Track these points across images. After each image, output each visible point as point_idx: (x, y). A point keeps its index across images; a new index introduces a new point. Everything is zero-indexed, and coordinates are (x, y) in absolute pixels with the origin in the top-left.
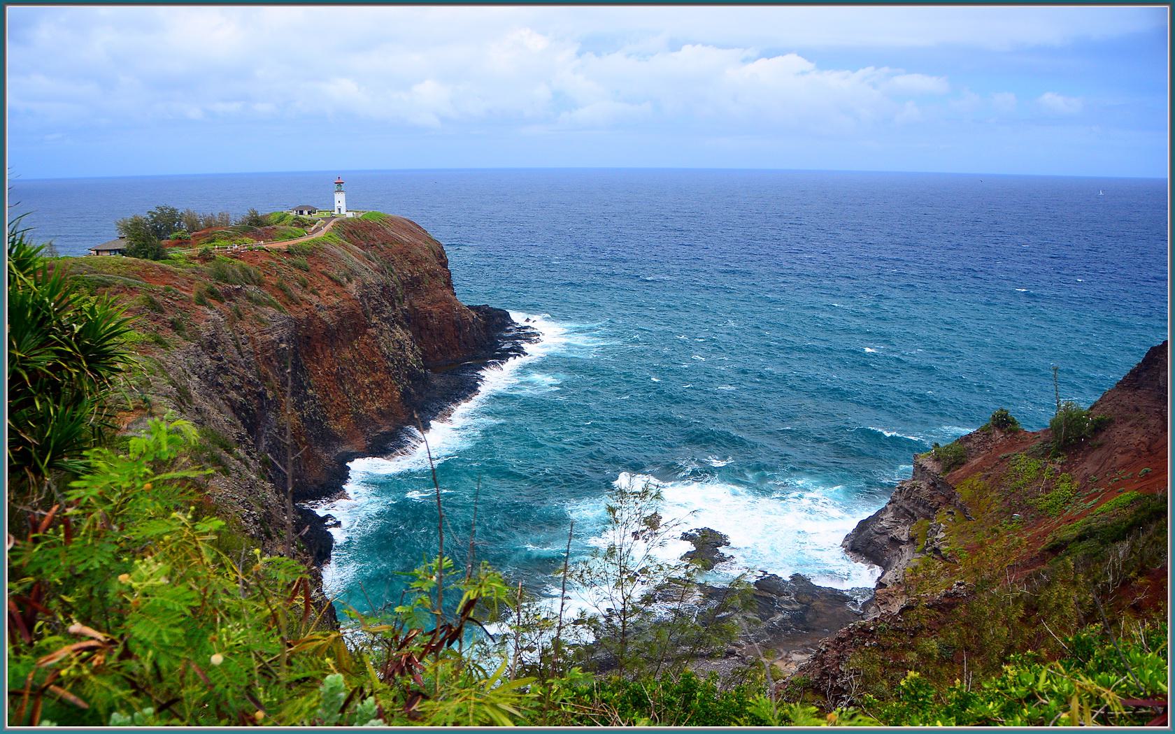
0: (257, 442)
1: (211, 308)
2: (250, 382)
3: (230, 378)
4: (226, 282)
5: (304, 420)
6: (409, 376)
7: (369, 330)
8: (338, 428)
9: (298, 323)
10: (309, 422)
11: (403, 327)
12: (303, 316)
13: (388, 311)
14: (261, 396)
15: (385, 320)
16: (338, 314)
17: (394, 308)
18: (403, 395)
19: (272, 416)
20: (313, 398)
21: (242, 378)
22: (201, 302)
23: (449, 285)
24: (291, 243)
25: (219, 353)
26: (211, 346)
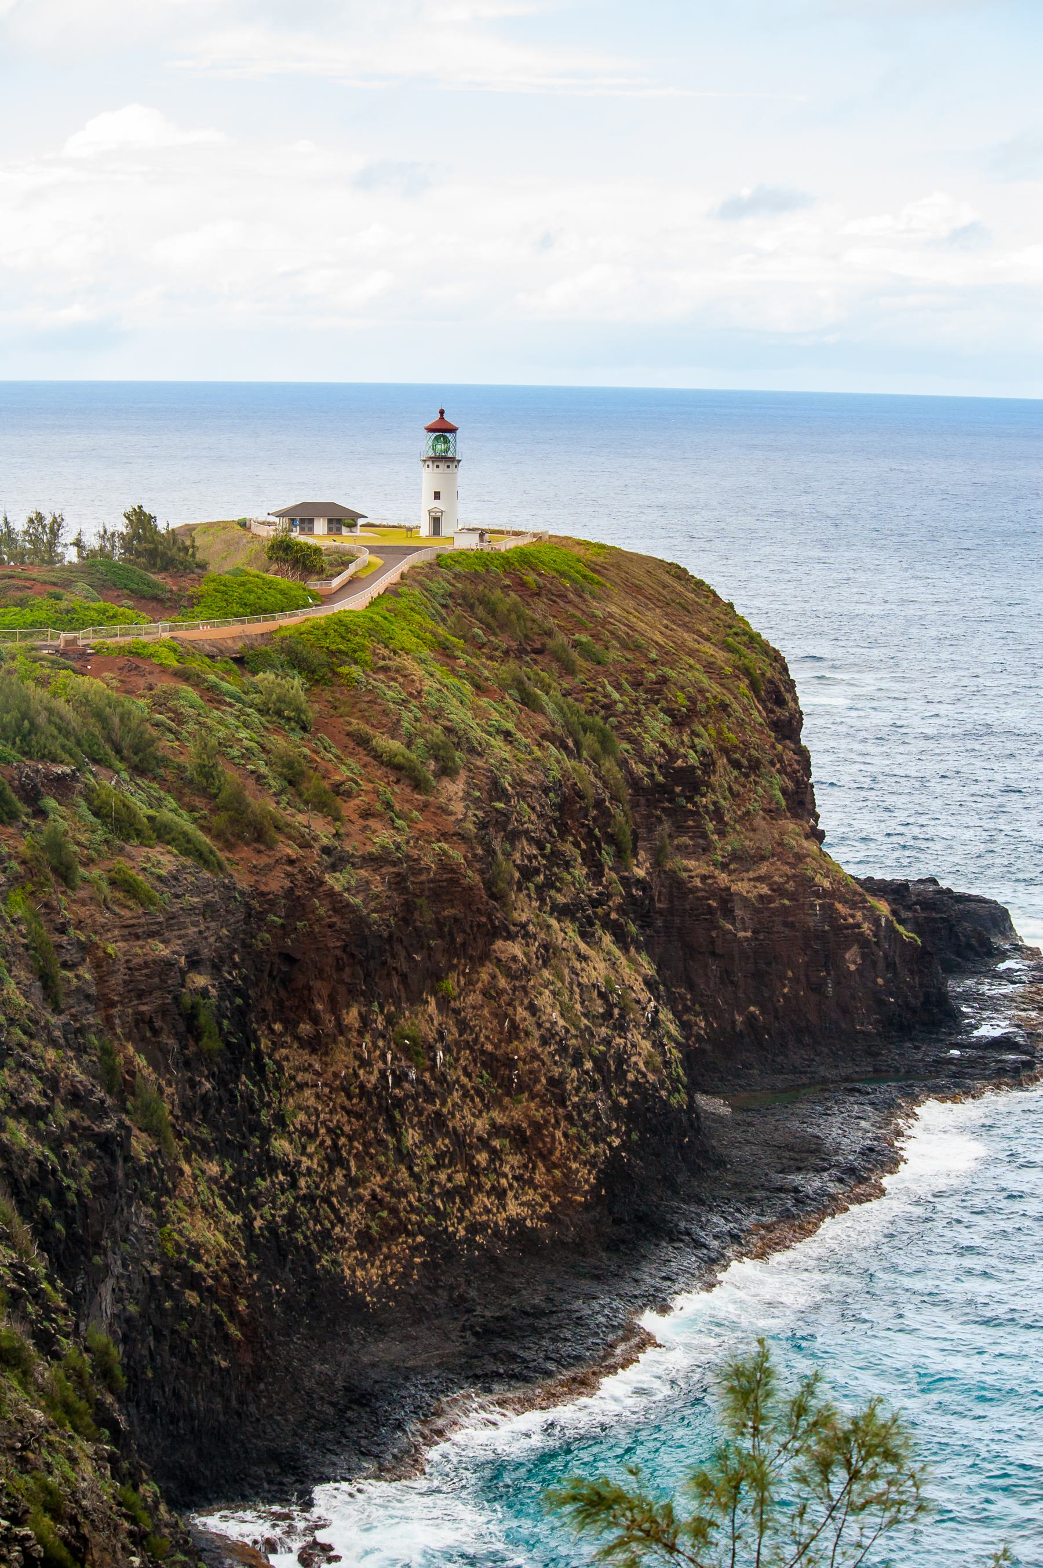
0: (79, 1302)
2: (76, 1098)
5: (253, 1242)
6: (630, 1115)
9: (254, 910)
10: (272, 1248)
11: (621, 939)
12: (276, 883)
14: (109, 1147)
15: (562, 912)
16: (398, 883)
19: (141, 1216)
20: (292, 1171)
21: (51, 1082)
23: (800, 800)
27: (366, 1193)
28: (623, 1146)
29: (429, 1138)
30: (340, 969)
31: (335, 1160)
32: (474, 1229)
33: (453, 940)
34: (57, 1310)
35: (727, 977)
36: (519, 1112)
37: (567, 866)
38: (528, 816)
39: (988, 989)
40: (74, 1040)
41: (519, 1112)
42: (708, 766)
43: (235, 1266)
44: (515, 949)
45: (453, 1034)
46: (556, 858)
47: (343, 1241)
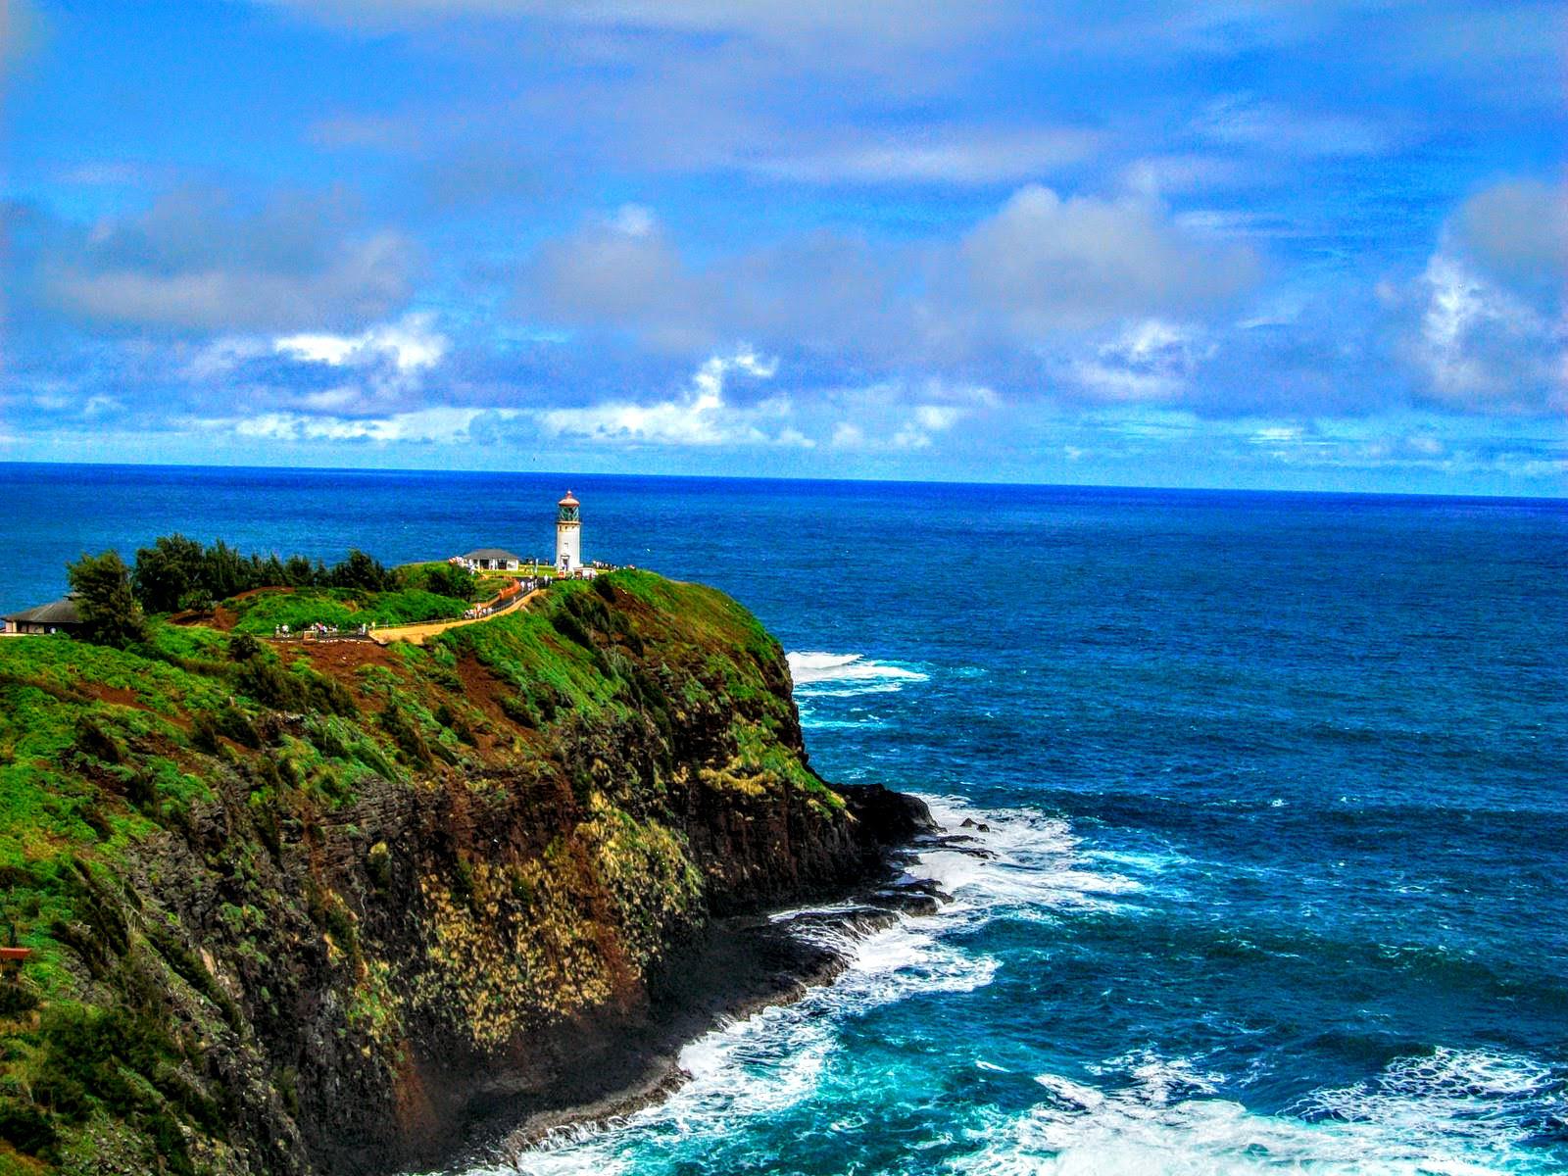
1: (227, 758)
2: (290, 926)
4: (271, 705)
6: (665, 934)
10: (424, 1020)
11: (663, 821)
14: (312, 957)
17: (648, 780)
20: (440, 969)
27: (490, 982)
28: (659, 952)
29: (532, 947)
30: (476, 841)
32: (560, 1005)
33: (550, 824)
34: (254, 1063)
35: (737, 848)
37: (629, 776)
38: (603, 743)
40: (291, 889)
42: (729, 717)
43: (396, 1030)
44: (594, 827)
47: (474, 1013)
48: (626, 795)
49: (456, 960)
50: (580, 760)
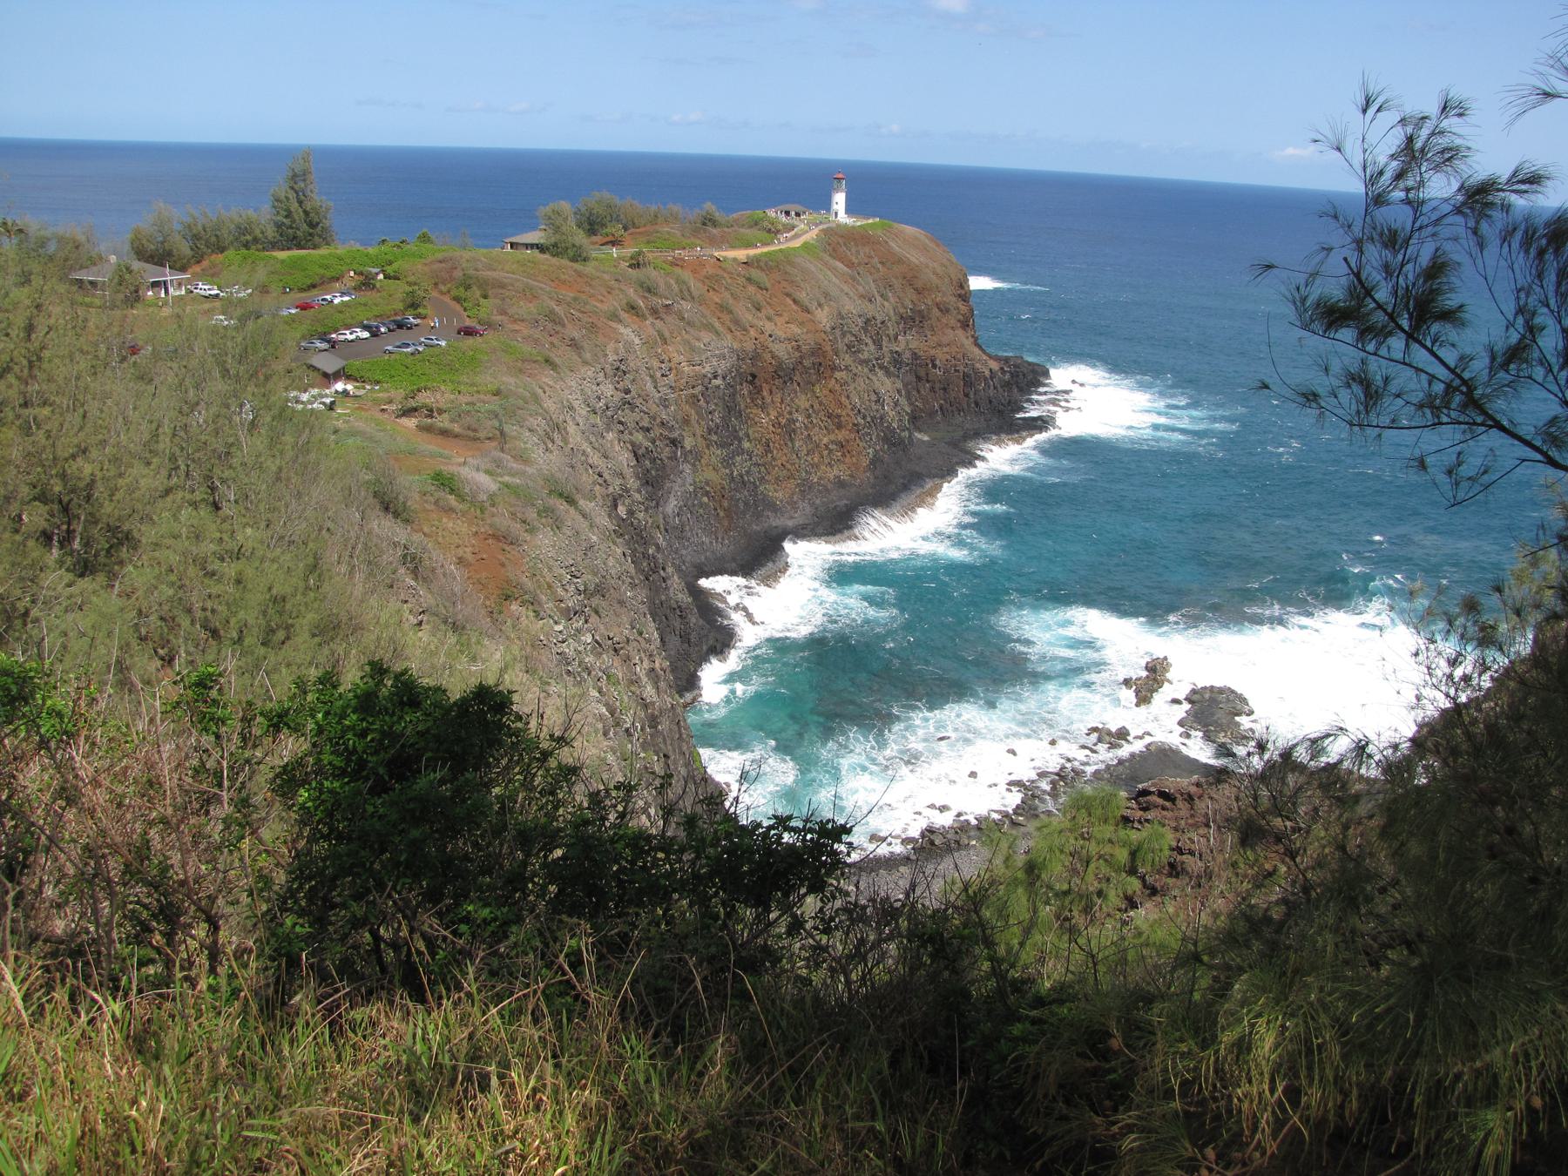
3: (636, 416)
6: (886, 440)
7: (838, 375)
8: (779, 495)
11: (888, 373)
12: (749, 346)
13: (869, 350)
18: (873, 462)
22: (614, 317)
24: (752, 252)
25: (627, 383)
26: (619, 371)
31: (768, 449)
35: (932, 389)
36: (841, 435)
39: (1035, 397)
41: (841, 435)
45: (816, 406)
46: (860, 341)
48: (865, 356)
49: (759, 450)
50: (838, 332)
